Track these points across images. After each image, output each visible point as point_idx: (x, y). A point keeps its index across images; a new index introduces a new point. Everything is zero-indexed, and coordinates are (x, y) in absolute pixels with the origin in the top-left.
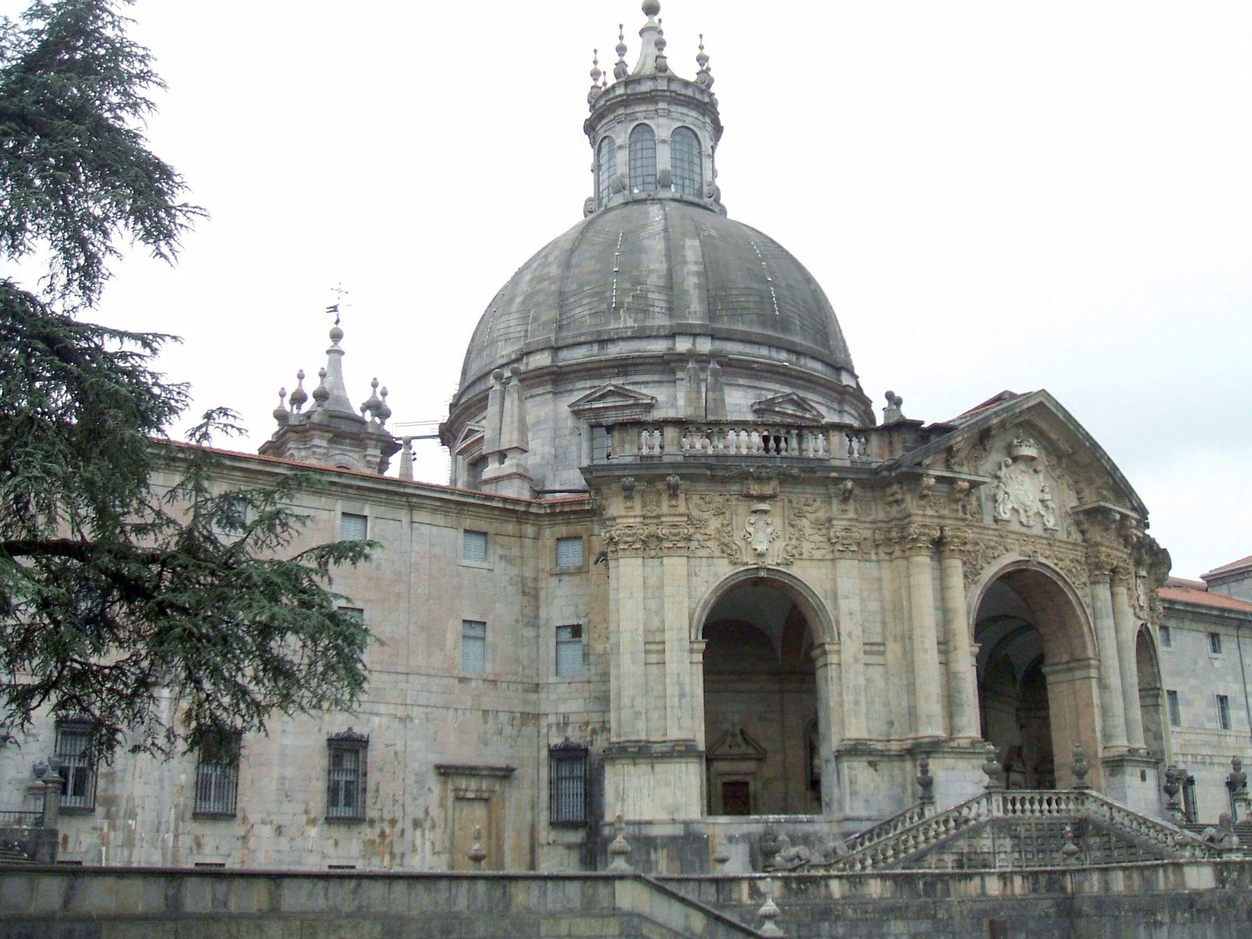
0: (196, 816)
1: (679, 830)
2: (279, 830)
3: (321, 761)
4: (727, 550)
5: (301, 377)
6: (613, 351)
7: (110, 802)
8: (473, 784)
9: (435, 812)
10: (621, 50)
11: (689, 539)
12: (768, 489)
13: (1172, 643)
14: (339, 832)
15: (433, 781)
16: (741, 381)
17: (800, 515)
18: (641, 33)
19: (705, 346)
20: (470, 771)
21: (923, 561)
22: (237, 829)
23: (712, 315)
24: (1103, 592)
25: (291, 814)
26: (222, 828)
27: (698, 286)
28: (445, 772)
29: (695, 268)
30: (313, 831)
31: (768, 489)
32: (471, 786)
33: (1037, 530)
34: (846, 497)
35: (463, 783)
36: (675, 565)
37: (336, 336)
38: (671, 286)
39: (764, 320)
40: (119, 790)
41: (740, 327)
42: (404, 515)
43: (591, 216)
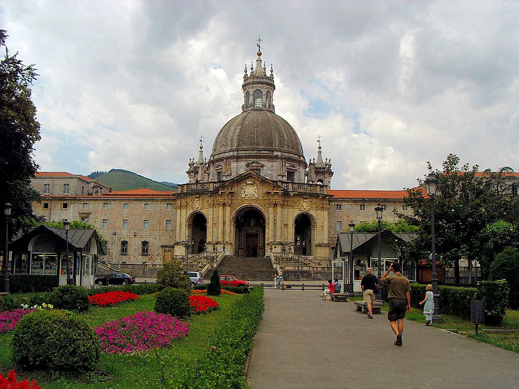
0: (121, 255)
1: (181, 257)
2: (134, 257)
3: (141, 245)
4: (193, 208)
5: (191, 160)
6: (221, 156)
7: (109, 253)
8: (167, 248)
9: (160, 253)
10: (246, 71)
11: (186, 206)
12: (198, 196)
13: (365, 209)
14: (143, 257)
15: (160, 248)
16: (244, 160)
17: (204, 200)
18: (257, 61)
19: (235, 153)
20: (166, 246)
21: (221, 208)
22: (128, 257)
23: (239, 145)
24: (271, 210)
25: (136, 254)
26: (126, 256)
27: (237, 139)
28: (162, 246)
29: (237, 134)
30: (140, 257)
31: (198, 196)
32: (167, 249)
33: (254, 198)
34: (210, 196)
35: (166, 248)
36: (184, 211)
37: (201, 148)
38: (232, 140)
39: (252, 143)
40: (111, 251)
41: (245, 147)
42: (155, 203)
43: (246, 114)
